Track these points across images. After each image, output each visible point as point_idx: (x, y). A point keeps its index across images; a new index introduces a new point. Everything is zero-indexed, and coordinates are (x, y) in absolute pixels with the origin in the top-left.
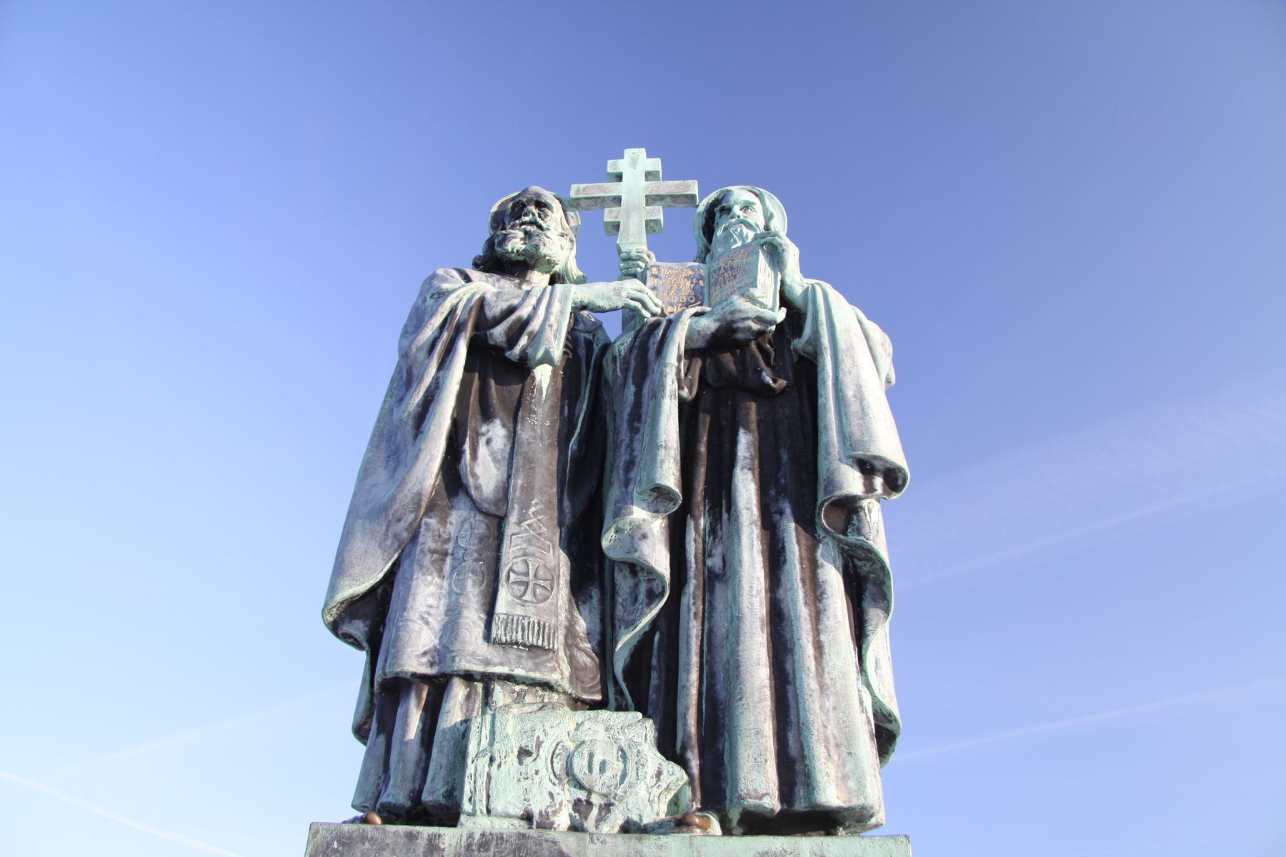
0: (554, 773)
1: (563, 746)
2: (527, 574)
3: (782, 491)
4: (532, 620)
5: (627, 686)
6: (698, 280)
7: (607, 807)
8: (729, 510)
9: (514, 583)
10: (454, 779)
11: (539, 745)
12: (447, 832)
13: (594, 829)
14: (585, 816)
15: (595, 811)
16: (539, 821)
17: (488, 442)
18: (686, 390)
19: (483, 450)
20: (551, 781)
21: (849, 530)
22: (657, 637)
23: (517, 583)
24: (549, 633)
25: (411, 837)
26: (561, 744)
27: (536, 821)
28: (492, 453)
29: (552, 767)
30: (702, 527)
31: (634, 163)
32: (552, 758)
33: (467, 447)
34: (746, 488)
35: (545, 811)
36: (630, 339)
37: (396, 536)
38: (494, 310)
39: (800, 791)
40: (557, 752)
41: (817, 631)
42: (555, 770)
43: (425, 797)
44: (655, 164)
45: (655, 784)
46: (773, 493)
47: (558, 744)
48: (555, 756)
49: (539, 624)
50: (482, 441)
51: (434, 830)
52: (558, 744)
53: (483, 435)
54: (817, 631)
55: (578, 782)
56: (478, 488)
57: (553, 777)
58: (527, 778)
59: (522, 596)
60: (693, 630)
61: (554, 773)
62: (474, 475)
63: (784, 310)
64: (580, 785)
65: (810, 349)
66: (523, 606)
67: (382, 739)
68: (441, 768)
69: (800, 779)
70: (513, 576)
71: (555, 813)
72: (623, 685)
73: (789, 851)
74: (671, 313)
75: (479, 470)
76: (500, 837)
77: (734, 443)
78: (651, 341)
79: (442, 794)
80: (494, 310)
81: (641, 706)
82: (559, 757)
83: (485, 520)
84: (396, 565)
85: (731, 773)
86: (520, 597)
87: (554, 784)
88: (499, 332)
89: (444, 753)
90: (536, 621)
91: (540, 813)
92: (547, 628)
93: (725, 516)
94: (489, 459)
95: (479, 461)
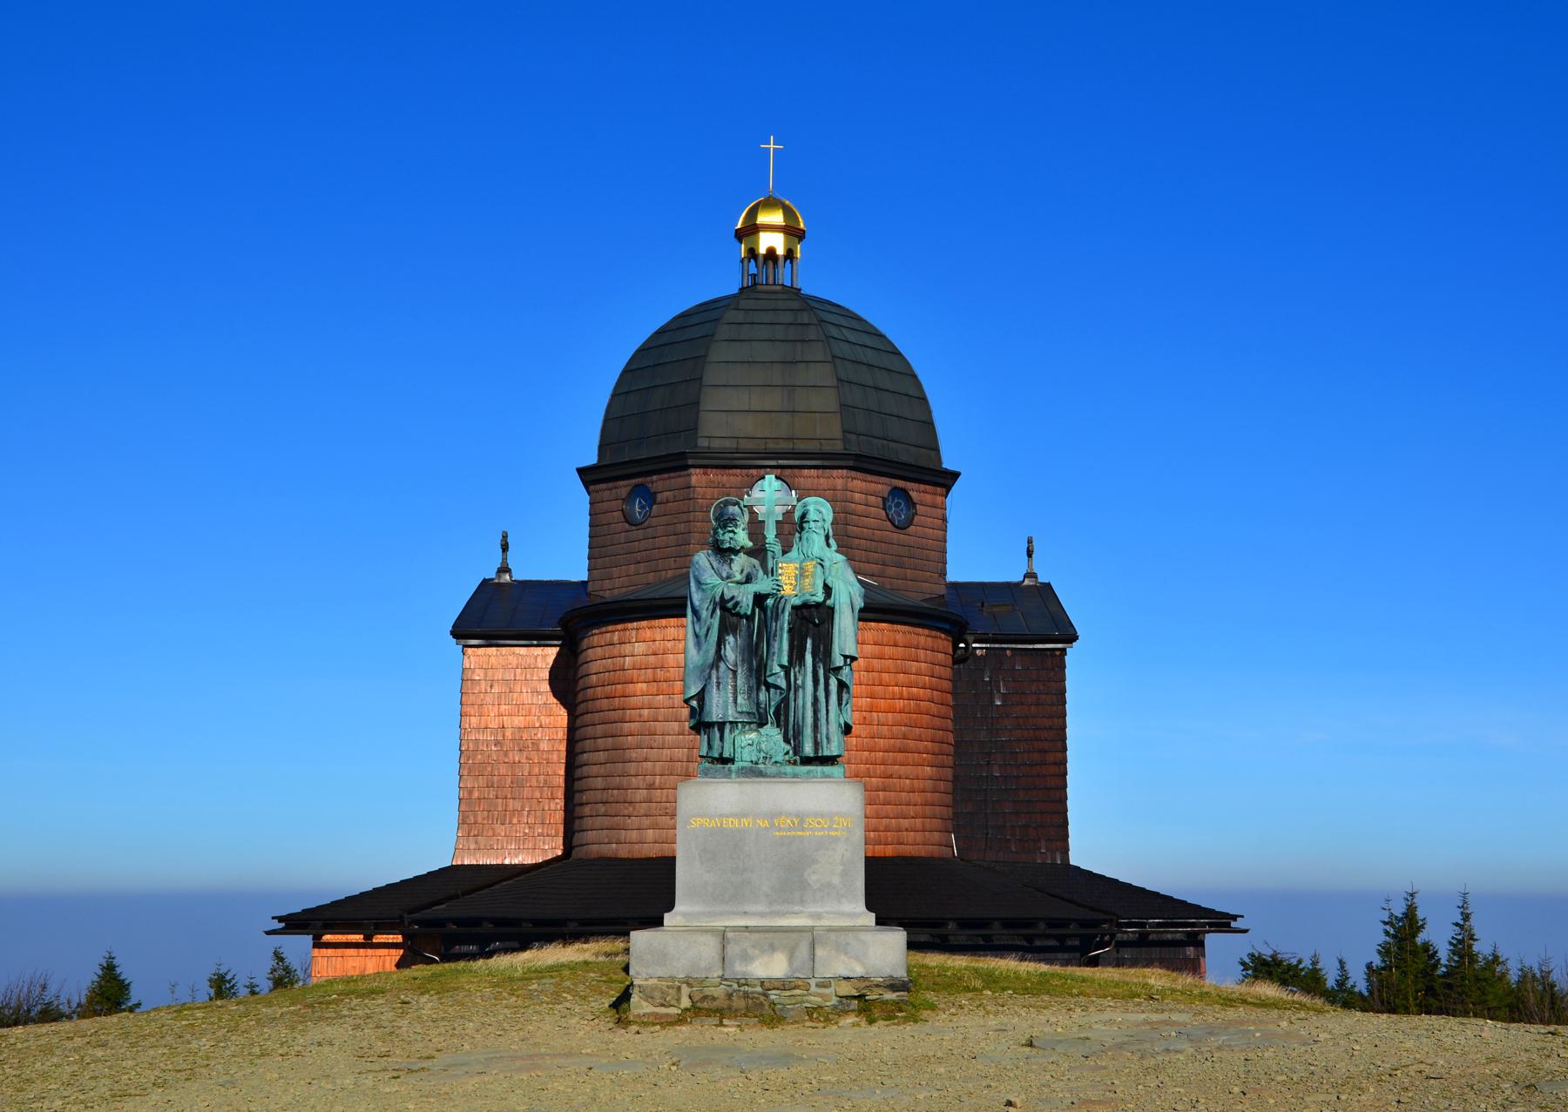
3: (820, 659)
7: (771, 758)
19: (727, 646)
34: (809, 658)
37: (704, 677)
38: (727, 597)
39: (820, 751)
41: (827, 706)
50: (727, 643)
54: (827, 706)
56: (728, 661)
69: (820, 748)
77: (806, 643)
80: (727, 597)
84: (705, 685)
85: (803, 714)
88: (730, 605)
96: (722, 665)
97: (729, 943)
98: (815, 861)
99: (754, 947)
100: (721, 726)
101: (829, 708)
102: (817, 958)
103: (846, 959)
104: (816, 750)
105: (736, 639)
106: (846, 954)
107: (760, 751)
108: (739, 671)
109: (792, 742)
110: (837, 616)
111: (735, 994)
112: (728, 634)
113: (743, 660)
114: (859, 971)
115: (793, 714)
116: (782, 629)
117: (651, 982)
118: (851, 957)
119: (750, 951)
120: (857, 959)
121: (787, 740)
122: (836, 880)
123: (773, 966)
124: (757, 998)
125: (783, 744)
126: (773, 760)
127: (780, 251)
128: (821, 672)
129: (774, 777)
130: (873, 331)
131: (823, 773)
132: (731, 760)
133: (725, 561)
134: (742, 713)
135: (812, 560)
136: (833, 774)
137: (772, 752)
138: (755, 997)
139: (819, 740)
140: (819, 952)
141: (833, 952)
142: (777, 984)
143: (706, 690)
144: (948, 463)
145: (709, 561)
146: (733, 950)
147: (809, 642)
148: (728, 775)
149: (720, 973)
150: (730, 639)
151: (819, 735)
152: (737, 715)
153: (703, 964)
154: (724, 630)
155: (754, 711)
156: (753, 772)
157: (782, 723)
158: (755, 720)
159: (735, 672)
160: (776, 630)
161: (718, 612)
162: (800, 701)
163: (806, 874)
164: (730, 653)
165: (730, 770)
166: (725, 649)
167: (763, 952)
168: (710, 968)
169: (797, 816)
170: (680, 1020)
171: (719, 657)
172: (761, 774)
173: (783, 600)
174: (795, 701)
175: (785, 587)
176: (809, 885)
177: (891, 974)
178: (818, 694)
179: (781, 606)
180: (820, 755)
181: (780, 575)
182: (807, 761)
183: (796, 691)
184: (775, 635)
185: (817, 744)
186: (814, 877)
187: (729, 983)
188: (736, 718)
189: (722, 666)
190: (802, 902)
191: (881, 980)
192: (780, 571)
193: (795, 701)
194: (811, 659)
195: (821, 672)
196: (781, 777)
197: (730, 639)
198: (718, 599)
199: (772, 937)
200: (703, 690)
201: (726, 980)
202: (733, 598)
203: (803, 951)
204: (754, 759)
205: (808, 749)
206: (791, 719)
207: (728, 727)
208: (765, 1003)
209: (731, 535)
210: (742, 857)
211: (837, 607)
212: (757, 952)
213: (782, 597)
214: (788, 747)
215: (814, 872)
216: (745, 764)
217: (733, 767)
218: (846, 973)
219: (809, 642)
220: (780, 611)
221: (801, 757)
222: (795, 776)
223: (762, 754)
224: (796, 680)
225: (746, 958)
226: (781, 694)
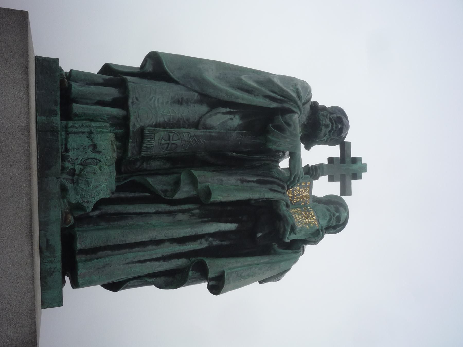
0: (86, 160)
1: (98, 162)
2: (173, 140)
4: (153, 144)
5: (128, 181)
6: (304, 202)
7: (73, 182)
8: (202, 222)
9: (169, 135)
10: (83, 117)
11: (99, 152)
12: (58, 118)
13: (63, 178)
14: (68, 174)
15: (70, 177)
16: (65, 155)
17: (231, 119)
18: (254, 202)
20: (83, 159)
21: (193, 272)
22: (148, 194)
23: (169, 136)
24: (148, 151)
25: (55, 103)
26: (99, 162)
27: (65, 154)
28: (226, 122)
29: (89, 159)
30: (195, 211)
32: (93, 158)
33: (228, 110)
35: (69, 158)
36: (277, 176)
39: (83, 257)
40: (95, 160)
41: (151, 260)
42: (87, 160)
43: (74, 105)
45: (83, 201)
46: (210, 239)
47: (99, 160)
48: (93, 159)
49: (152, 147)
50: (231, 116)
51: (59, 113)
52: (99, 160)
53: (234, 117)
55: (83, 170)
56: (210, 116)
57: (84, 159)
58: (83, 149)
59: (163, 139)
60: (151, 208)
61: (86, 160)
62: (216, 114)
63: (289, 241)
64: (82, 171)
65: (273, 252)
66: (159, 140)
67: (102, 81)
68: (87, 111)
69: (89, 257)
70: (171, 135)
71: (69, 162)
72: (128, 180)
73: (55, 259)
74: (289, 193)
75: (219, 116)
77: (231, 222)
78: (275, 186)
79: (76, 112)
81: (119, 189)
82: (93, 161)
83: (196, 120)
86: (162, 138)
87: (81, 160)
89: (94, 111)
90: (153, 146)
91: (69, 156)
92: (150, 150)
93: (200, 220)
94: (224, 120)
95: (222, 116)
101: (148, 263)
105: (236, 129)
107: (84, 164)
108: (198, 132)
109: (97, 213)
110: (265, 259)
112: (242, 118)
113: (211, 138)
115: (138, 211)
116: (251, 189)
121: (103, 202)
125: (94, 201)
126: (69, 185)
129: (40, 189)
137: (82, 185)
139: (100, 254)
143: (172, 85)
150: (236, 121)
151: (109, 252)
155: (143, 154)
157: (123, 195)
158: (130, 155)
159: (196, 125)
160: (249, 182)
161: (274, 105)
162: (154, 220)
165: (52, 113)
166: (224, 113)
173: (280, 189)
174: (157, 213)
175: (290, 191)
178: (167, 244)
179: (275, 187)
180: (78, 258)
181: (301, 184)
183: (170, 213)
184: (242, 181)
189: (204, 109)
192: (303, 184)
193: (157, 213)
197: (236, 121)
198: (287, 106)
202: (289, 125)
204: (72, 155)
206: (131, 209)
211: (275, 258)
214: (89, 207)
217: (57, 120)
220: (269, 186)
221: (72, 227)
222: (43, 225)
223: (78, 168)
224: (183, 212)
226: (165, 191)
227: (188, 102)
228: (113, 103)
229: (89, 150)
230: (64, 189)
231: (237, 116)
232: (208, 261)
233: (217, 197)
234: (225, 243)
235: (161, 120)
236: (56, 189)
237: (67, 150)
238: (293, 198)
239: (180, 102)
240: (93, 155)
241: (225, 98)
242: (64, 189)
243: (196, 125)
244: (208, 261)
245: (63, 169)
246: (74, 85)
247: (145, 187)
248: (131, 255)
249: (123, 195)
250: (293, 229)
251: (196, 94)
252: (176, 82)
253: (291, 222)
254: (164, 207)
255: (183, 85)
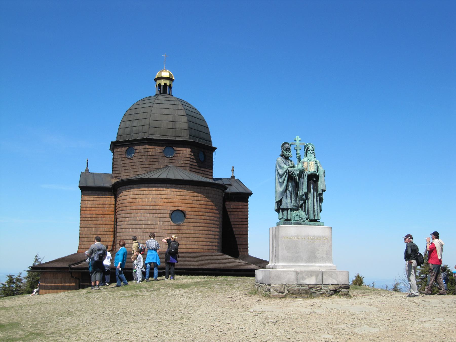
19: (289, 186)
25: (290, 222)
31: (298, 139)
34: (312, 190)
39: (315, 218)
44: (299, 139)
56: (289, 190)
76: (296, 222)
84: (283, 197)
96: (288, 192)
97: (298, 274)
98: (318, 250)
99: (306, 275)
100: (287, 210)
102: (323, 279)
103: (332, 279)
104: (314, 217)
106: (332, 277)
111: (301, 289)
114: (335, 282)
117: (276, 285)
118: (333, 278)
119: (305, 276)
120: (335, 279)
122: (325, 256)
123: (311, 281)
124: (307, 290)
126: (303, 220)
127: (168, 85)
128: (315, 195)
129: (304, 225)
130: (193, 108)
131: (318, 224)
132: (290, 220)
133: (287, 161)
134: (293, 206)
135: (313, 161)
136: (321, 224)
137: (303, 218)
138: (306, 290)
140: (324, 277)
141: (328, 277)
142: (312, 286)
144: (214, 145)
145: (283, 160)
146: (300, 276)
147: (312, 185)
148: (291, 224)
149: (296, 283)
152: (292, 206)
153: (291, 280)
154: (288, 182)
156: (298, 223)
157: (304, 209)
161: (287, 175)
163: (316, 254)
164: (290, 188)
165: (291, 223)
167: (308, 277)
168: (293, 281)
169: (313, 237)
170: (285, 297)
171: (286, 189)
172: (300, 224)
175: (305, 169)
176: (317, 257)
177: (344, 283)
178: (314, 201)
182: (311, 221)
185: (314, 216)
186: (318, 255)
187: (299, 286)
188: (292, 207)
190: (315, 262)
191: (342, 285)
194: (312, 191)
195: (315, 195)
196: (306, 225)
197: (290, 184)
199: (311, 273)
200: (282, 199)
201: (298, 285)
203: (320, 276)
204: (298, 219)
205: (311, 217)
207: (289, 211)
208: (309, 292)
209: (288, 153)
210: (298, 249)
212: (307, 277)
213: (305, 172)
215: (318, 253)
216: (296, 221)
218: (332, 283)
219: (312, 185)
222: (310, 225)
225: (304, 278)
227: (287, 195)
228: (288, 211)
229: (297, 216)
230: (304, 221)
231: (289, 183)
232: (318, 193)
233: (306, 191)
234: (315, 187)
235: (291, 202)
236: (304, 223)
237: (297, 220)
238: (307, 168)
239: (287, 197)
240: (298, 216)
241: (285, 187)
242: (304, 221)
243: (291, 193)
244: (318, 193)
245: (300, 221)
246: (284, 218)
247: (302, 204)
248: (316, 209)
249: (304, 209)
250: (315, 172)
251: (285, 193)
252: (283, 197)
253: (313, 172)
254: (307, 201)
255: (283, 196)
